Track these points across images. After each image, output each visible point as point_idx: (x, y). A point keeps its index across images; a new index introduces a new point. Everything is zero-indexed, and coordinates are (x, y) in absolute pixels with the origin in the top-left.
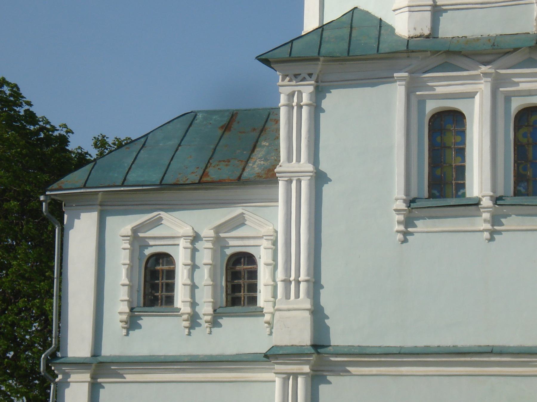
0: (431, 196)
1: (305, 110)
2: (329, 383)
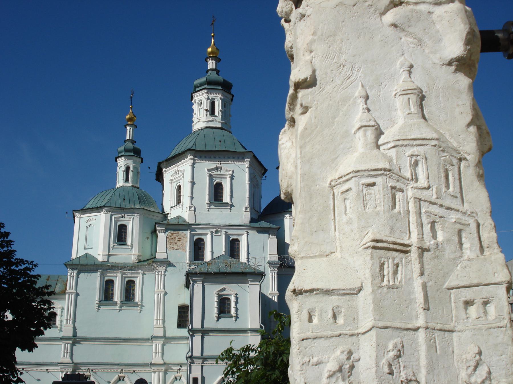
0: (105, 300)
1: (75, 277)
2: (76, 346)
